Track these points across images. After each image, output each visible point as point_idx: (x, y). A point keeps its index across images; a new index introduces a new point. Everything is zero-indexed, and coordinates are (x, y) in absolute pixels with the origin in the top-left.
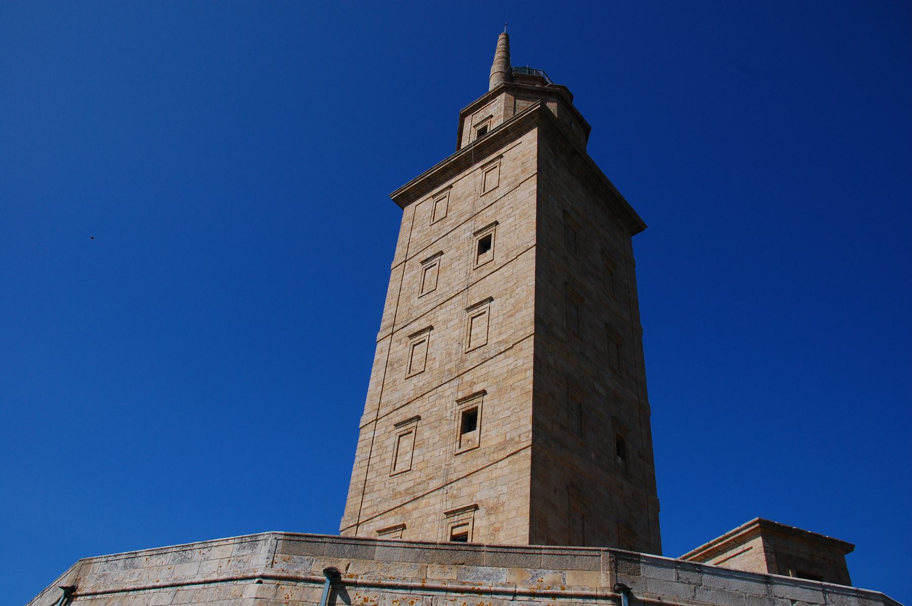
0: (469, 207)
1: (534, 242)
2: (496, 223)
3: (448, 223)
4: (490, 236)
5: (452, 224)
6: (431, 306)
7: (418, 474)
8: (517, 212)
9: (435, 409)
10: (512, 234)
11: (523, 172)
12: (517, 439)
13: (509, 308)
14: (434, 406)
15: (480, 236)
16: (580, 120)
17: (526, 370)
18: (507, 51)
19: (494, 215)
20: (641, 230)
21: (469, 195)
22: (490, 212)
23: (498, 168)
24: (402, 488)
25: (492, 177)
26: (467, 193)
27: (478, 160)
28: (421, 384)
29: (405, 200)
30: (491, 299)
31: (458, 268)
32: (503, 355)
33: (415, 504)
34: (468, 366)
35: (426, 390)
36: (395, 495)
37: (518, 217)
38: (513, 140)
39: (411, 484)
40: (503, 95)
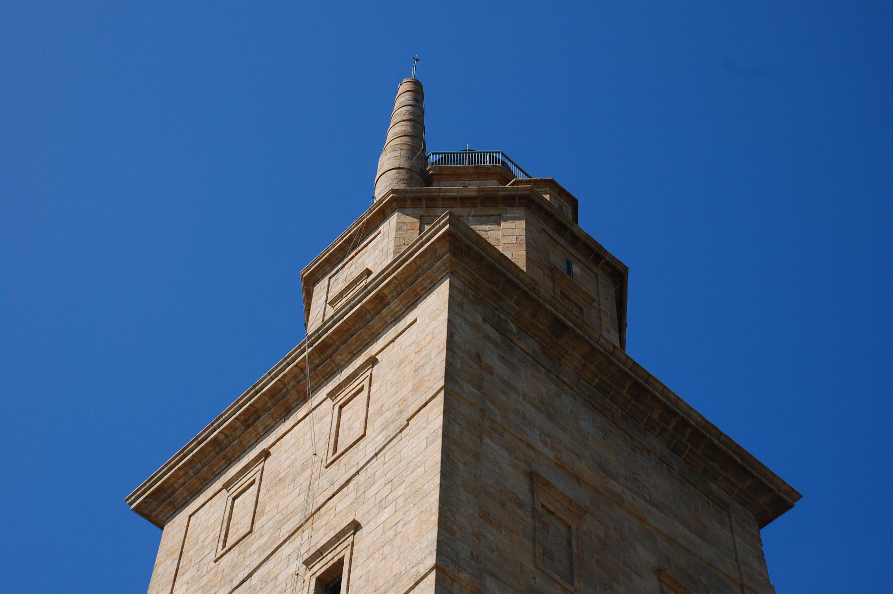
0: (302, 498)
1: (431, 561)
2: (355, 526)
3: (254, 548)
4: (340, 562)
8: (401, 490)
10: (387, 549)
11: (416, 389)
15: (320, 568)
16: (594, 254)
18: (417, 119)
20: (789, 506)
21: (303, 468)
22: (341, 503)
23: (364, 395)
25: (354, 413)
26: (298, 464)
29: (161, 505)
37: (401, 502)
38: (397, 319)
40: (394, 220)
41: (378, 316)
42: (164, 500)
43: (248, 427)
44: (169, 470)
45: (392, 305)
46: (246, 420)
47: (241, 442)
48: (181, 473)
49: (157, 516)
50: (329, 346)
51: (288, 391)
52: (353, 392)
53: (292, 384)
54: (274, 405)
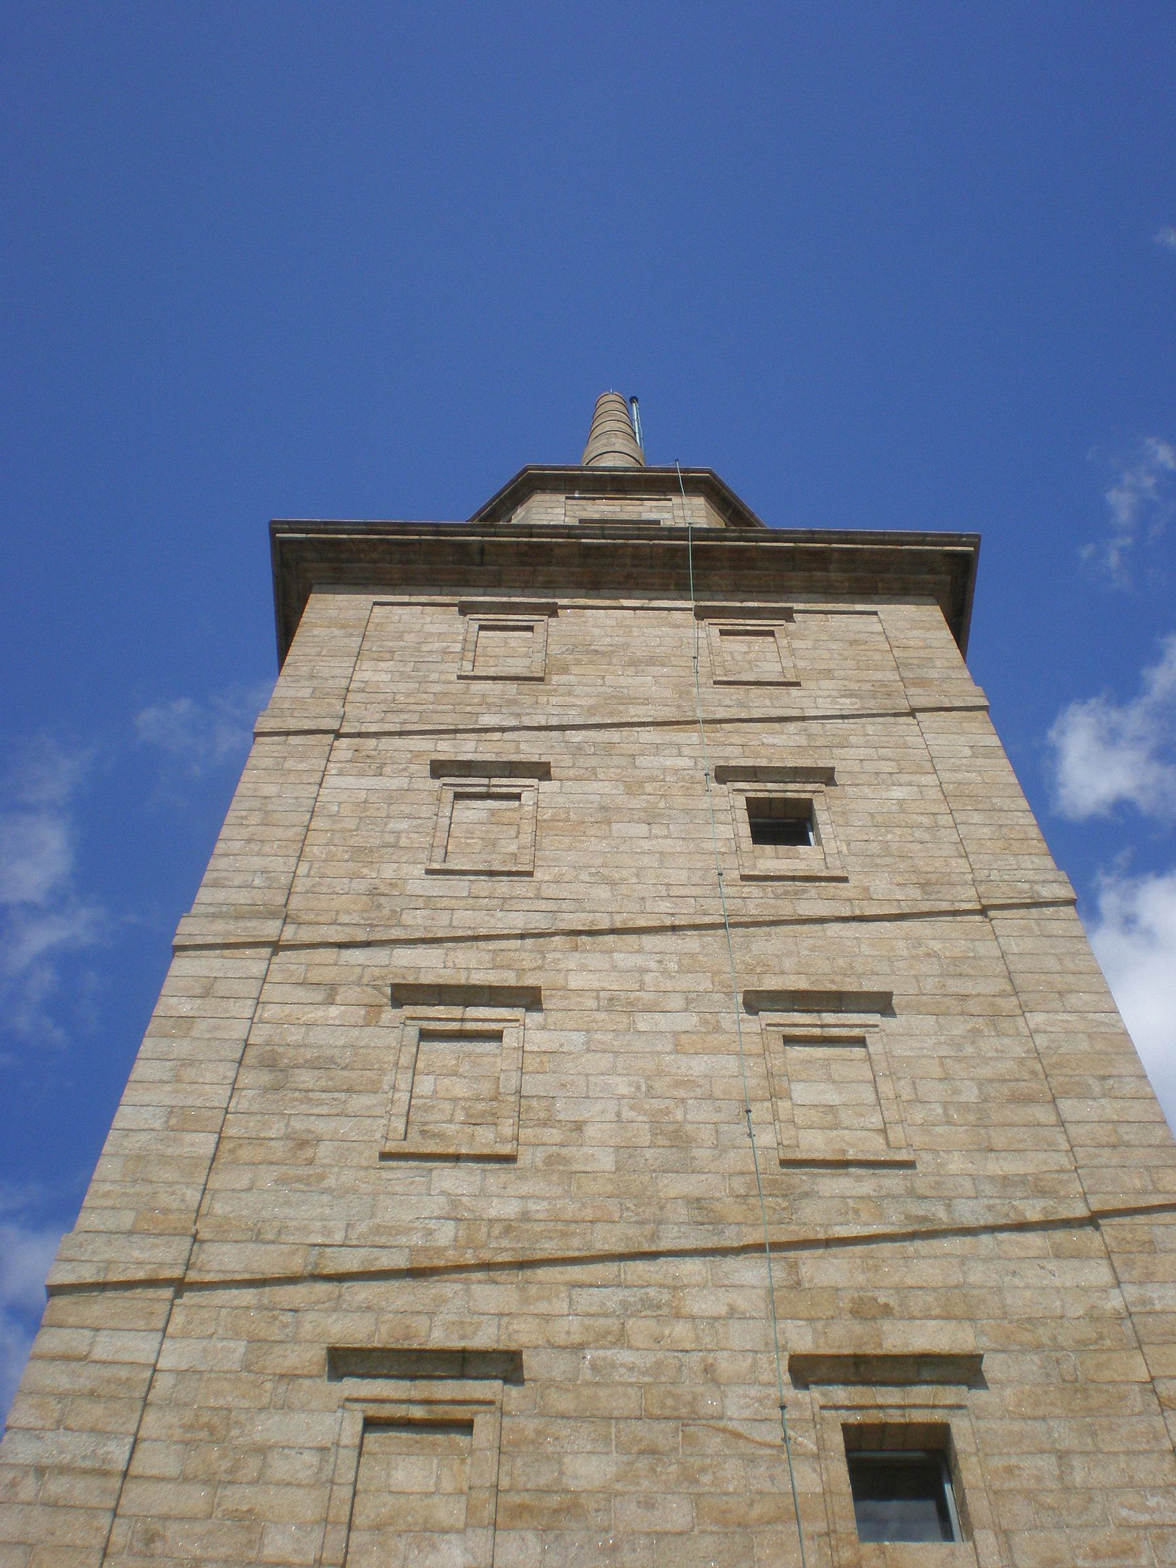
5: (591, 710)
6: (517, 921)
9: (625, 1356)
14: (621, 1339)
28: (510, 1209)
30: (882, 1003)
31: (646, 845)
32: (1035, 1240)
34: (813, 1218)
35: (549, 1248)
41: (807, 574)
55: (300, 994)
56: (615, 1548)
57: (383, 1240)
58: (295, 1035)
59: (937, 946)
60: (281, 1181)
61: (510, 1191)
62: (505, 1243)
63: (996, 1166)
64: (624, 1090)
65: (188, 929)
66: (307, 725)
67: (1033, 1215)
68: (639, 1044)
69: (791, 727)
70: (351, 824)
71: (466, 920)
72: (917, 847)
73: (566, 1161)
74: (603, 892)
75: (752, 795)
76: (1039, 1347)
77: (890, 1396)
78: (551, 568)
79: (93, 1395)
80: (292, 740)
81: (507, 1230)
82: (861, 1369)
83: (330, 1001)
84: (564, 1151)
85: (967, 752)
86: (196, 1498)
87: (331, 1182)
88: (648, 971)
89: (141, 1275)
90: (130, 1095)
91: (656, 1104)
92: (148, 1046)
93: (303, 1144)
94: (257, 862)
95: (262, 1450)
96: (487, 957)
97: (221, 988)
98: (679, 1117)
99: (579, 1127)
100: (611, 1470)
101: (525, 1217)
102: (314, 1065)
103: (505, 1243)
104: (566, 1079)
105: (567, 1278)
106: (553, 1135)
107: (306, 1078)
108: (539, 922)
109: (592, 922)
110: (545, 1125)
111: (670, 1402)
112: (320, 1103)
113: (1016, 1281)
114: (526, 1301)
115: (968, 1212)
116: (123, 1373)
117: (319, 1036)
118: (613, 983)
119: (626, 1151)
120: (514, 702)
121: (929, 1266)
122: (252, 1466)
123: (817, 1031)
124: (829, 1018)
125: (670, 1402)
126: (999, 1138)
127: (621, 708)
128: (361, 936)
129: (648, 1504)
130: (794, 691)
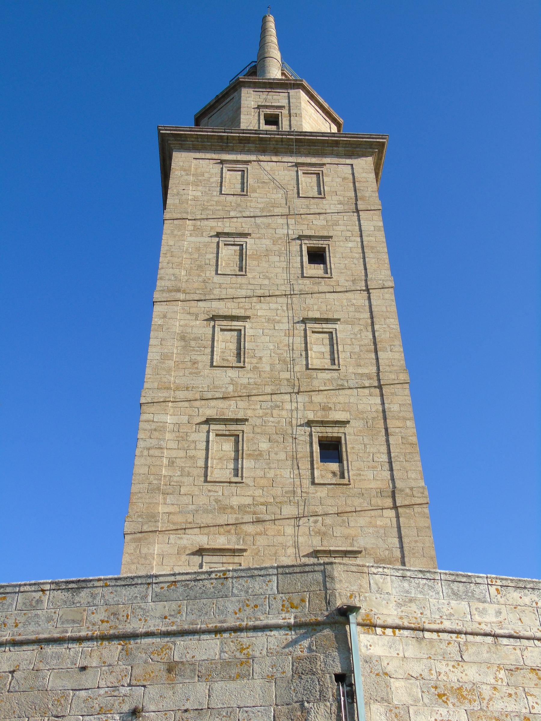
5: (262, 210)
6: (243, 293)
7: (258, 492)
9: (271, 419)
12: (408, 491)
13: (366, 342)
17: (405, 419)
19: (323, 227)
24: (235, 501)
27: (299, 153)
28: (245, 381)
33: (259, 528)
36: (223, 509)
39: (249, 501)
41: (331, 148)
42: (179, 140)
43: (241, 143)
44: (190, 131)
45: (340, 149)
46: (241, 140)
47: (233, 146)
48: (195, 136)
49: (170, 144)
50: (302, 142)
51: (269, 144)
52: (312, 172)
53: (273, 143)
54: (259, 144)
55: (188, 317)
56: (270, 463)
57: (216, 390)
58: (189, 330)
59: (354, 301)
60: (190, 373)
61: (245, 376)
62: (244, 391)
63: (360, 371)
64: (272, 347)
65: (157, 296)
66: (179, 216)
67: (367, 385)
68: (276, 334)
69: (322, 217)
70: (196, 256)
71: (231, 292)
72: (354, 266)
73: (258, 368)
74: (266, 282)
75: (309, 245)
76: (363, 419)
77: (329, 430)
78: (250, 145)
79: (155, 430)
80: (176, 222)
81: (245, 387)
82: (323, 423)
83: (196, 319)
84: (257, 365)
85: (372, 228)
86: (182, 454)
87: (202, 373)
88: (278, 309)
89: (162, 400)
90: (150, 349)
91: (279, 351)
92: (152, 334)
93: (194, 363)
94: (171, 271)
95: (194, 442)
96: (236, 305)
97: (169, 316)
98: (285, 356)
99: (261, 358)
100: (269, 446)
101: (249, 384)
102: (194, 339)
103: (244, 391)
104: (258, 344)
105: (259, 399)
106: (255, 361)
107: (193, 343)
108: (250, 293)
109: (264, 293)
110: (252, 358)
111: (281, 430)
112: (197, 351)
113: (361, 402)
114: (250, 405)
115: (351, 384)
116: (161, 424)
117: (195, 330)
118: (269, 313)
119: (272, 365)
120: (239, 205)
121: (342, 397)
122: (192, 446)
123: (321, 330)
124: (324, 326)
125: (281, 430)
126: (362, 363)
127: (272, 209)
128: (203, 298)
129: (276, 454)
130: (324, 201)
